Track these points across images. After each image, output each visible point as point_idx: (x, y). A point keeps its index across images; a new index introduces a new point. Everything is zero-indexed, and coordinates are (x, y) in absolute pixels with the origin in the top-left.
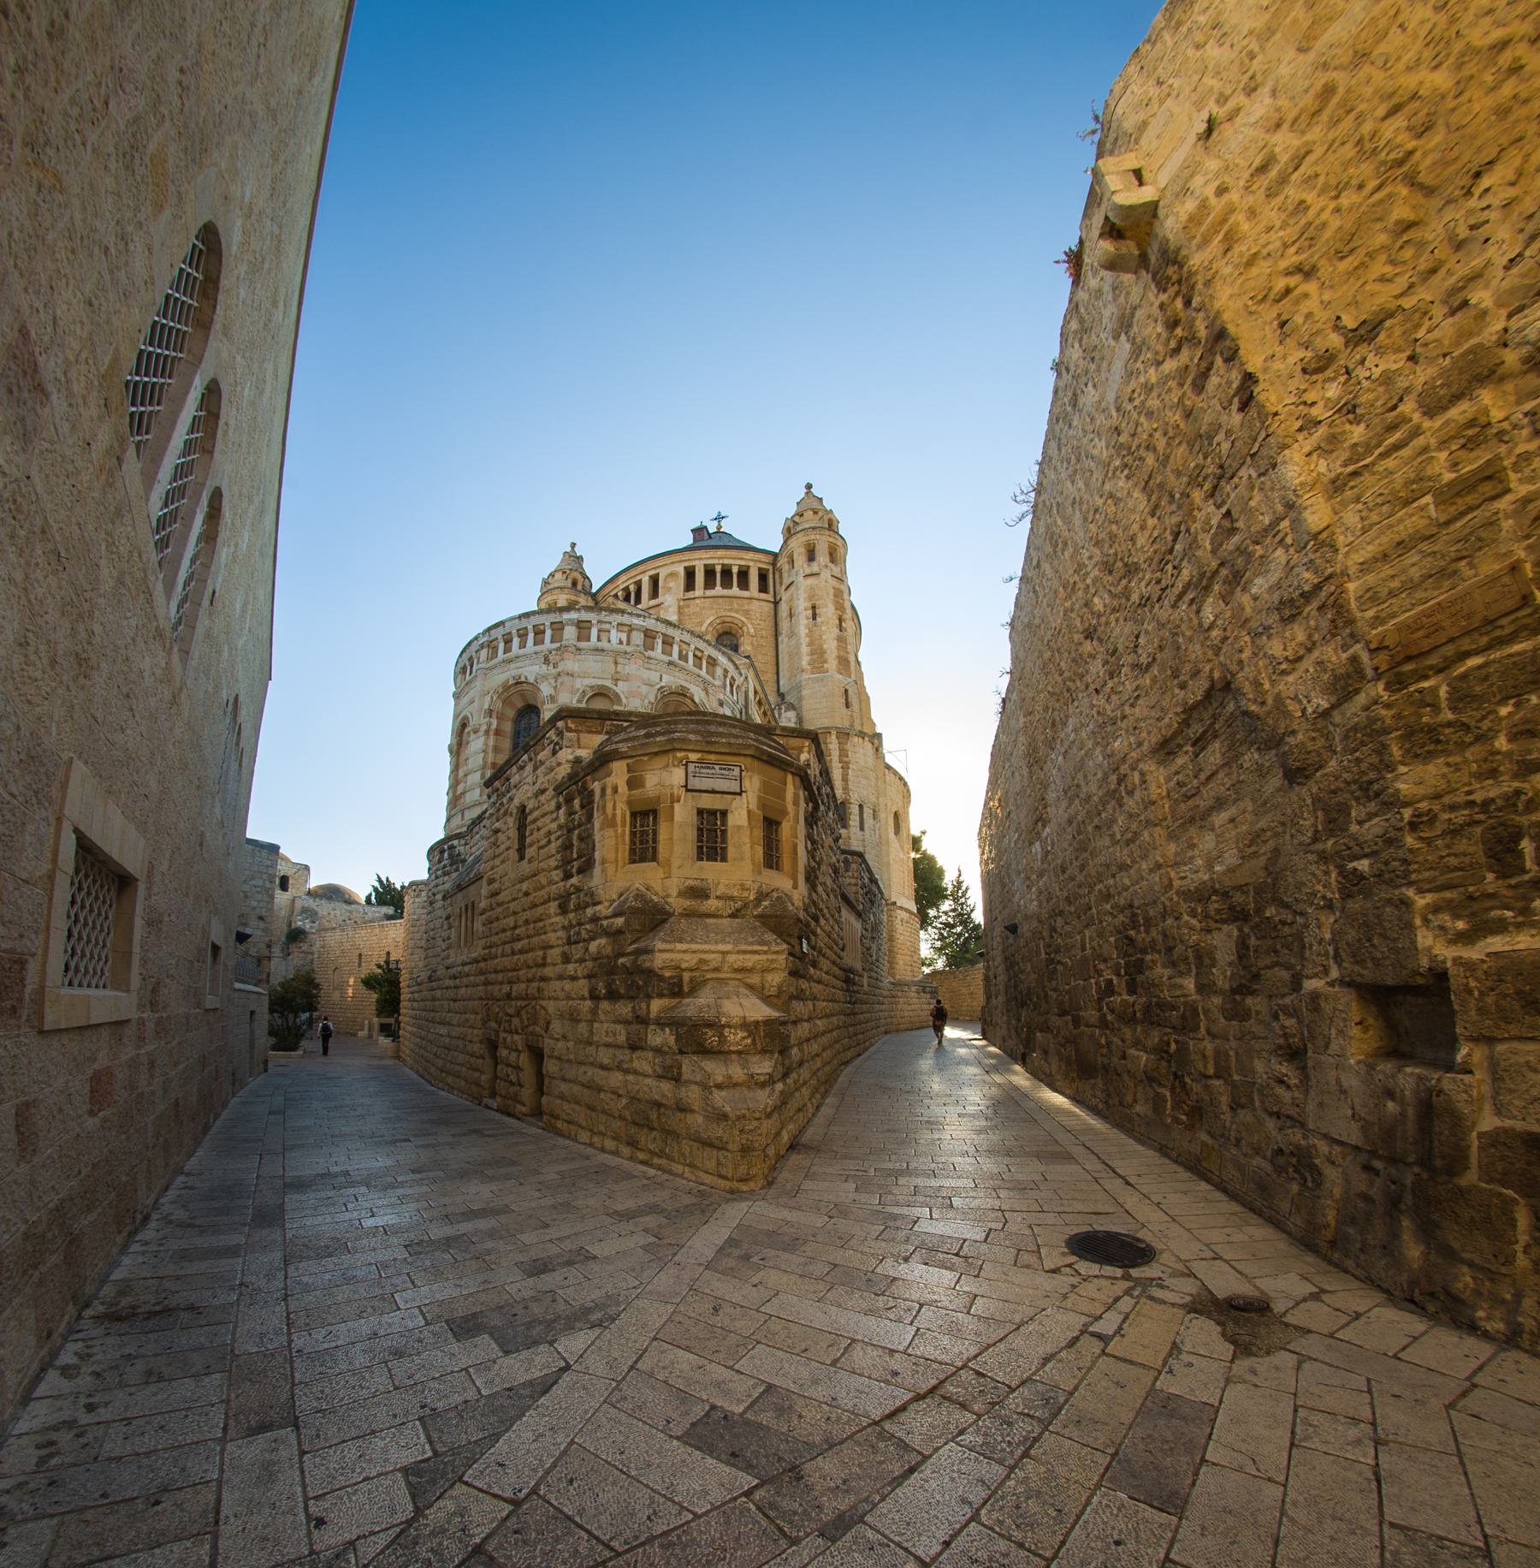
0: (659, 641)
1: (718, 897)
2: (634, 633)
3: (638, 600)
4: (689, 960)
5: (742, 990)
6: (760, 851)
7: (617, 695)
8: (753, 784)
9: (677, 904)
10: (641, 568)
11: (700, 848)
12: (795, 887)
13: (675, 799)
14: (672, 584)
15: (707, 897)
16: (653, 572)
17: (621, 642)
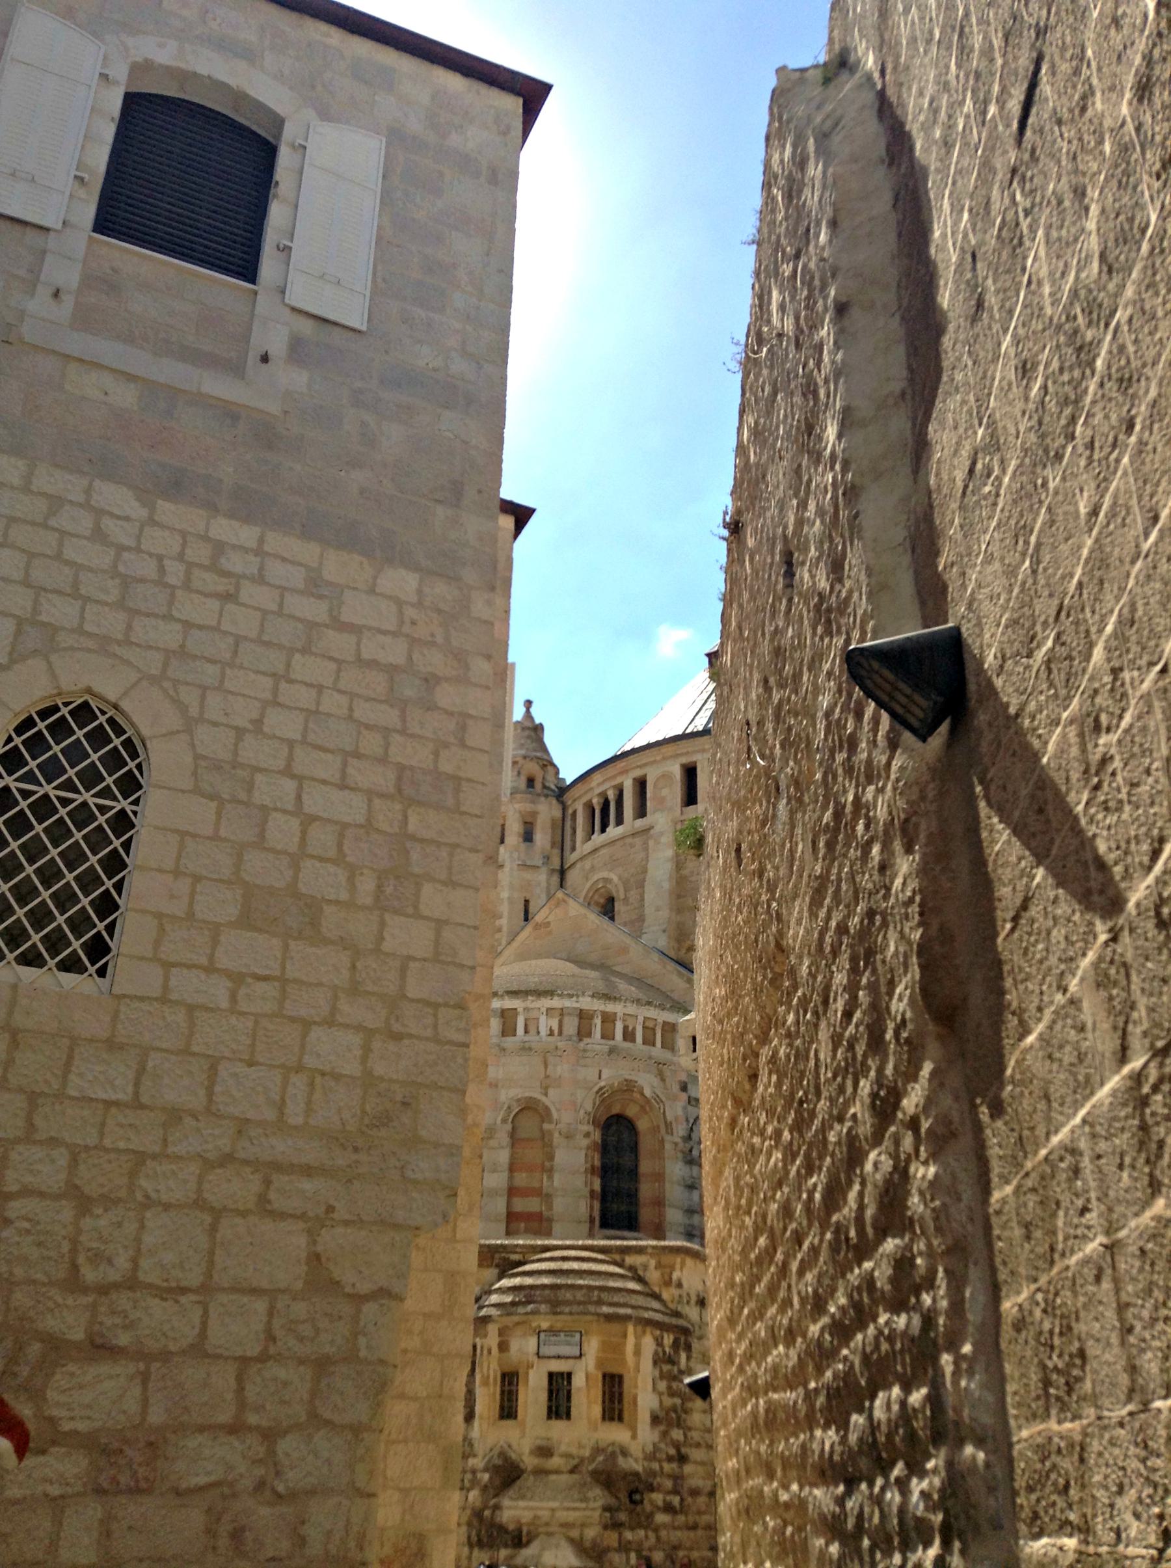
0: (598, 1021)
1: (562, 1456)
2: (566, 1019)
3: (620, 821)
4: (526, 1516)
5: (564, 1543)
6: (597, 1410)
7: (547, 1109)
8: (592, 1347)
9: (529, 1462)
10: (621, 765)
11: (550, 1408)
12: (634, 1437)
13: (530, 1366)
14: (665, 792)
15: (551, 1455)
16: (638, 773)
17: (551, 1033)
